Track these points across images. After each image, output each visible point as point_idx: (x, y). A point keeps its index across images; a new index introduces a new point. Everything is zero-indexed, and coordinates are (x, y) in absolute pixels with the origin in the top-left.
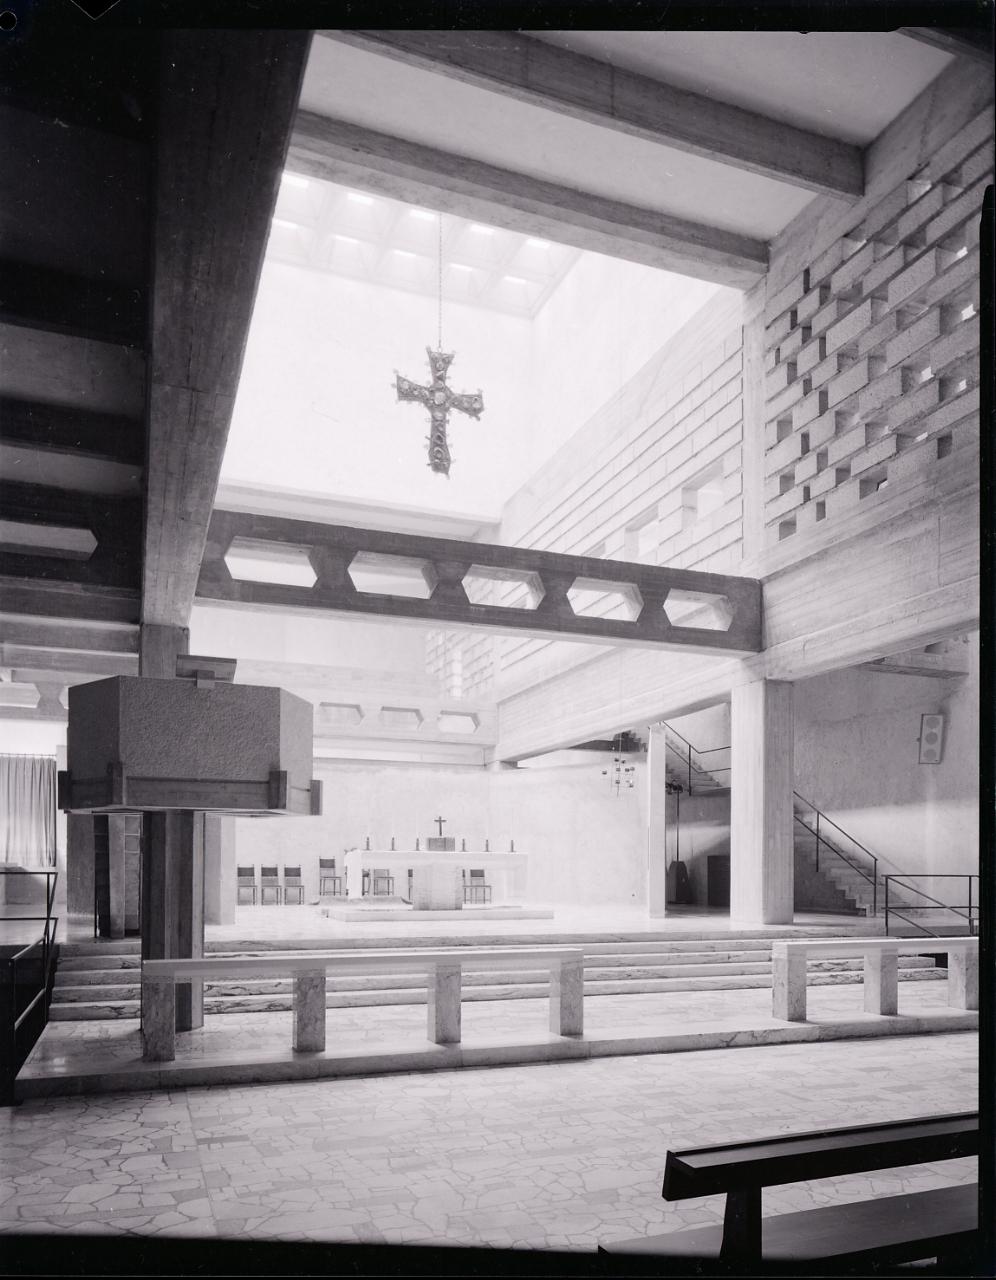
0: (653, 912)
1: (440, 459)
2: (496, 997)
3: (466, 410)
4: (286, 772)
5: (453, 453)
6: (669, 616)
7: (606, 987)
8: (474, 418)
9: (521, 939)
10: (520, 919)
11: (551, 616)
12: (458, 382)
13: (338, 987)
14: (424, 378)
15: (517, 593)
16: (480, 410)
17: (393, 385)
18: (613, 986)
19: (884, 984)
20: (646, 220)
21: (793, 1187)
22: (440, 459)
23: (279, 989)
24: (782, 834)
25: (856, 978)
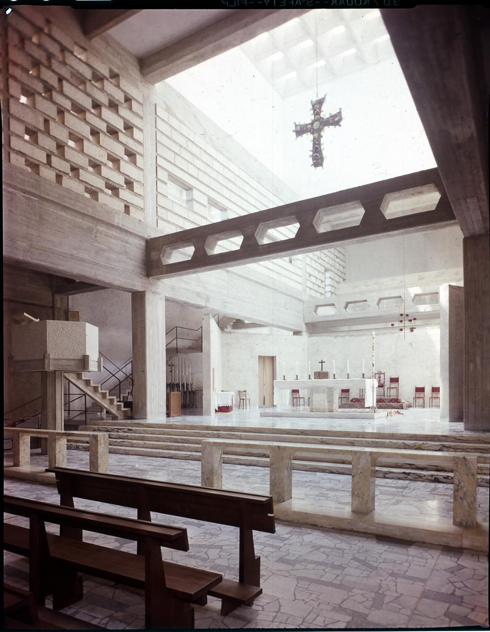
0: (442, 417)
1: (318, 159)
2: (181, 458)
3: (332, 124)
4: (88, 356)
5: (324, 153)
6: (242, 240)
7: (236, 459)
8: (337, 127)
9: (246, 429)
10: (352, 418)
11: (202, 261)
12: (307, 118)
13: (135, 445)
14: (325, 114)
15: (233, 243)
16: (340, 119)
17: (294, 131)
18: (240, 460)
19: (273, 477)
20: (115, 60)
21: (392, 625)
22: (318, 159)
23: (116, 444)
24: (482, 359)
25: (430, 478)
